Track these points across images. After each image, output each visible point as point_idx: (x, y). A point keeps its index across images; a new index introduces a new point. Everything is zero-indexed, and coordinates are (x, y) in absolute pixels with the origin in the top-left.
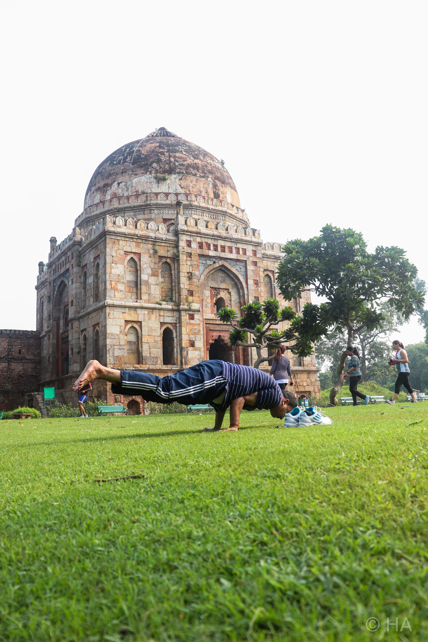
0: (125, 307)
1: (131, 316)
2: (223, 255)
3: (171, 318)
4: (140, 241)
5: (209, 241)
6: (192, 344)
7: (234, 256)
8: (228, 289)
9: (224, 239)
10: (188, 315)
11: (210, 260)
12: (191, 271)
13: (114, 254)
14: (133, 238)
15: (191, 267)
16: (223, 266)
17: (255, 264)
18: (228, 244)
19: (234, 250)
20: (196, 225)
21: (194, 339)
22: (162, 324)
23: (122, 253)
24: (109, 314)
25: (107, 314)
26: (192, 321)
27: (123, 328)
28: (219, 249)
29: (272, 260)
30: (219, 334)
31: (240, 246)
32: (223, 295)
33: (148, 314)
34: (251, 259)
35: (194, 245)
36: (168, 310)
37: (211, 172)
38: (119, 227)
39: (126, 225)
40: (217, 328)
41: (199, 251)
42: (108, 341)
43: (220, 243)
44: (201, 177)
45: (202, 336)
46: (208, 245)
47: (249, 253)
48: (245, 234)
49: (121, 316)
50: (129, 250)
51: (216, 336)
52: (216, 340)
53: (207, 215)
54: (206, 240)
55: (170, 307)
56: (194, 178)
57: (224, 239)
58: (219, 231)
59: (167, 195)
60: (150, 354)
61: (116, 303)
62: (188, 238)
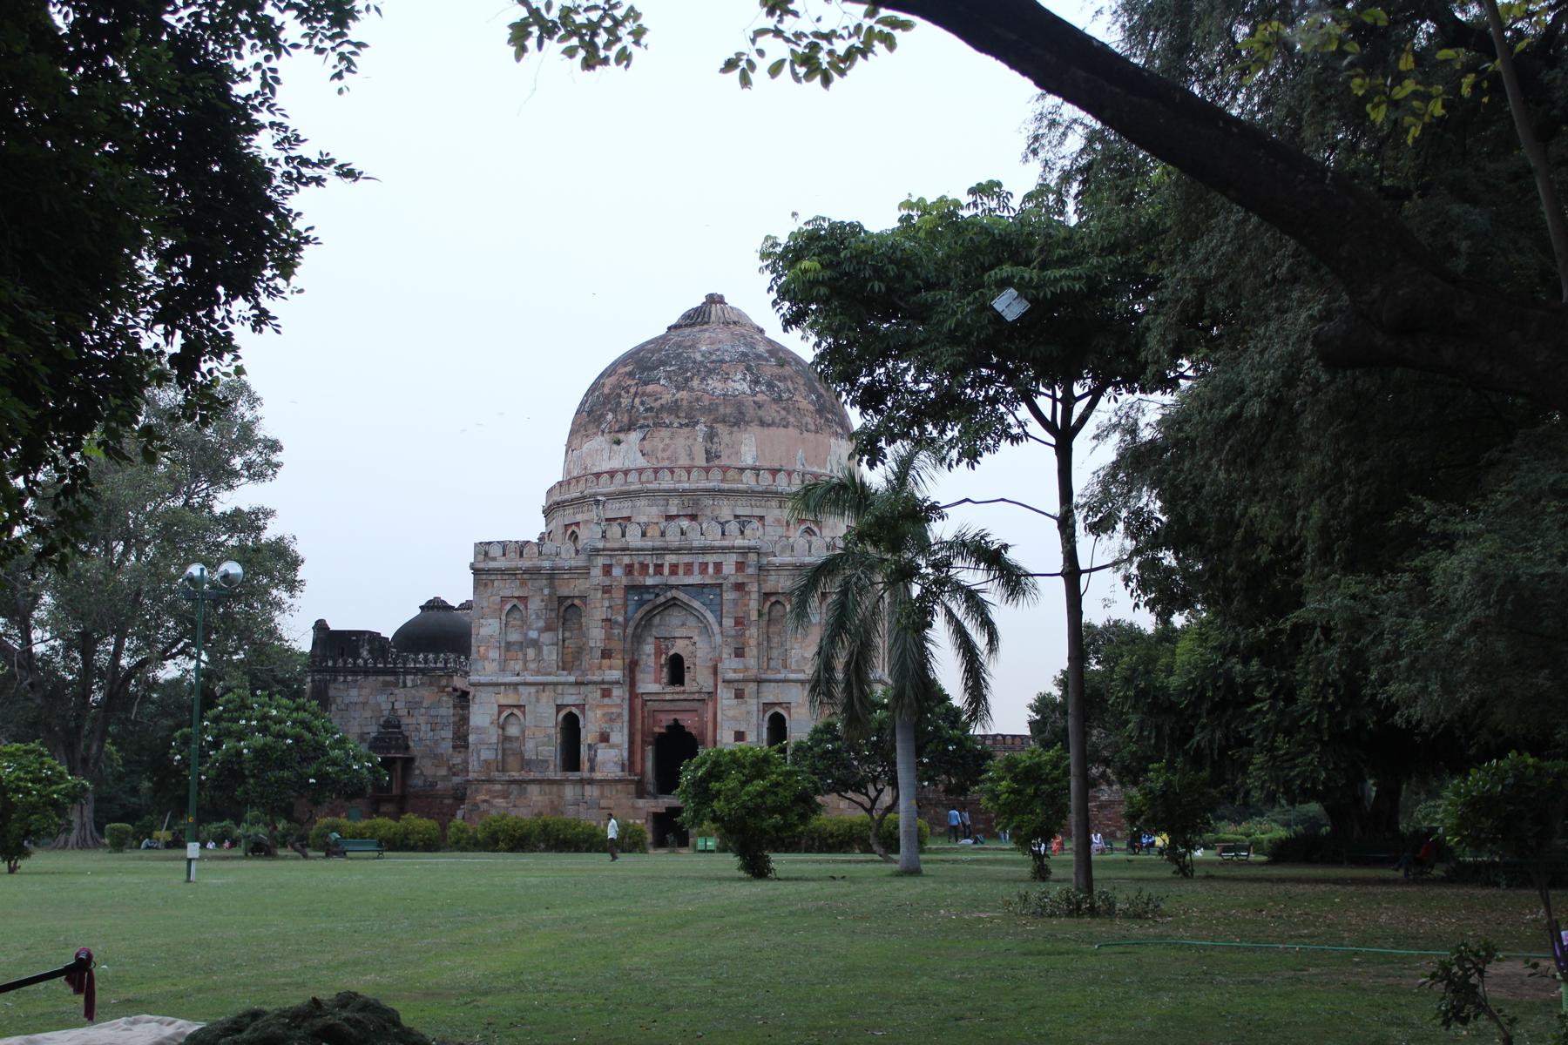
0: (498, 685)
1: (508, 698)
2: (673, 580)
5: (648, 560)
6: (604, 738)
7: (696, 579)
9: (677, 551)
13: (485, 604)
16: (674, 598)
17: (739, 587)
18: (687, 559)
19: (696, 569)
20: (623, 535)
22: (559, 708)
26: (606, 701)
28: (666, 571)
30: (673, 716)
31: (711, 559)
32: (680, 647)
34: (732, 580)
35: (617, 571)
36: (571, 684)
37: (703, 410)
38: (494, 559)
41: (625, 581)
42: (472, 738)
43: (670, 559)
44: (681, 425)
45: (626, 725)
46: (644, 567)
47: (729, 568)
48: (723, 533)
50: (507, 593)
55: (572, 679)
56: (665, 433)
57: (677, 551)
59: (612, 474)
61: (483, 679)
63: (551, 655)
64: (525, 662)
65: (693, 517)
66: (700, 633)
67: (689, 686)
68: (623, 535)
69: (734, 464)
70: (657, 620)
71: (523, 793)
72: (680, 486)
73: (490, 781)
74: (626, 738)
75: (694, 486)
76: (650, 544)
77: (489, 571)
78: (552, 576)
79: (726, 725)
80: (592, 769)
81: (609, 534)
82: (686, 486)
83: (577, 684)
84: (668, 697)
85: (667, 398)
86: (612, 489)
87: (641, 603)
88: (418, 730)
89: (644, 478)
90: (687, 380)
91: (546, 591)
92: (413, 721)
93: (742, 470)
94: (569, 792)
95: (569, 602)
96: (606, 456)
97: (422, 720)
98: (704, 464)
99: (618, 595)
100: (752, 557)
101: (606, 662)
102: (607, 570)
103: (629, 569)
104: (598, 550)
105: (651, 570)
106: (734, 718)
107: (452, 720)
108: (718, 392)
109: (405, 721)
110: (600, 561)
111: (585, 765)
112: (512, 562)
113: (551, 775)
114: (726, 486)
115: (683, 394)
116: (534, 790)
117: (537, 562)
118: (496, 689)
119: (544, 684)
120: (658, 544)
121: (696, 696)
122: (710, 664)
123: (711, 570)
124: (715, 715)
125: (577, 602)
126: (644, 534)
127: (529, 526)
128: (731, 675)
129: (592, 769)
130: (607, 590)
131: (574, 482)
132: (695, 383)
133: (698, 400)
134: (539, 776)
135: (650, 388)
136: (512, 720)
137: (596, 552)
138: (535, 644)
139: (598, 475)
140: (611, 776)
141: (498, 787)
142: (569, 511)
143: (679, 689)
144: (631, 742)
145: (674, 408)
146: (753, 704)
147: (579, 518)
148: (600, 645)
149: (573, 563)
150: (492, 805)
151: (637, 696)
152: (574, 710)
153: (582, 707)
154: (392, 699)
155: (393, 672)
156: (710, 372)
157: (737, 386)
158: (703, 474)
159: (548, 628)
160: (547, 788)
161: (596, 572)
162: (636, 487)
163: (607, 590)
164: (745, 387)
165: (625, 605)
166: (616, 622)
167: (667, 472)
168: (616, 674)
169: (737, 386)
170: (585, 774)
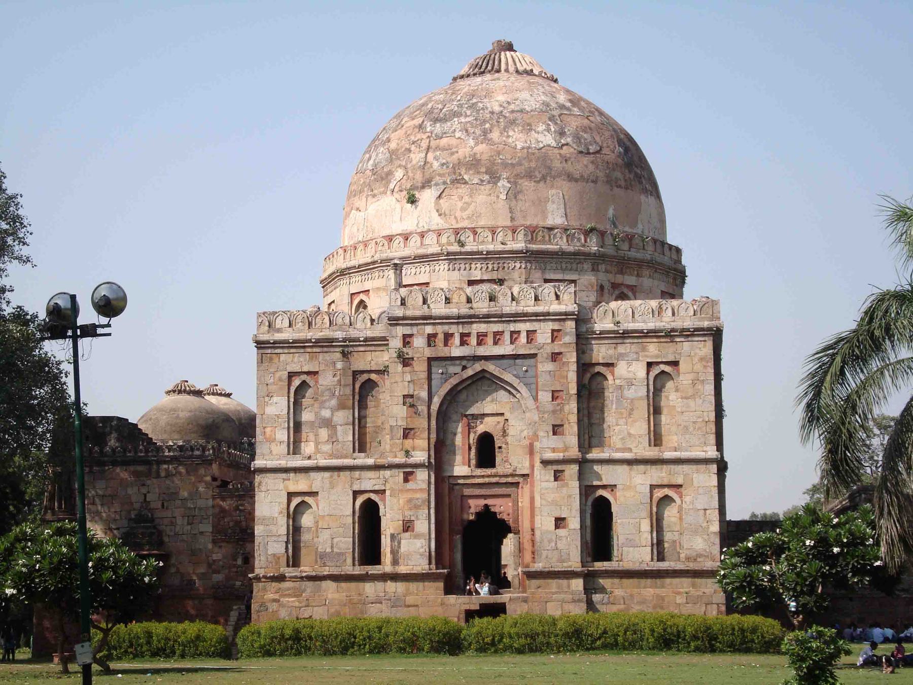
0: (286, 470)
1: (300, 484)
2: (482, 351)
3: (373, 482)
4: (318, 350)
6: (407, 526)
7: (505, 349)
8: (502, 414)
9: (486, 318)
10: (402, 475)
11: (455, 365)
12: (411, 393)
14: (304, 347)
15: (411, 385)
16: (483, 371)
17: (555, 357)
22: (356, 494)
23: (285, 375)
24: (260, 484)
25: (256, 484)
26: (410, 485)
27: (286, 506)
28: (473, 340)
29: (610, 341)
30: (482, 502)
31: (523, 327)
33: (331, 477)
34: (549, 349)
35: (419, 342)
39: (290, 325)
40: (478, 492)
41: (428, 352)
42: (258, 530)
43: (477, 328)
45: (433, 511)
48: (536, 299)
49: (281, 486)
50: (297, 369)
51: (476, 506)
52: (477, 514)
53: (479, 266)
54: (446, 328)
55: (370, 461)
56: (463, 190)
57: (486, 318)
58: (475, 305)
59: (406, 237)
60: (332, 547)
61: (270, 464)
62: (407, 330)
63: (346, 436)
64: (317, 444)
65: (501, 282)
66: (512, 409)
67: (500, 469)
68: (425, 301)
69: (541, 224)
70: (463, 396)
71: (319, 589)
72: (482, 248)
73: (281, 578)
75: (500, 247)
76: (453, 311)
77: (276, 344)
78: (347, 348)
81: (409, 302)
82: (491, 247)
83: (377, 467)
85: (464, 152)
86: (407, 252)
87: (446, 377)
88: (173, 524)
89: (444, 240)
90: (485, 133)
91: (339, 365)
92: (169, 514)
93: (551, 229)
94: (370, 589)
95: (365, 377)
96: (397, 218)
97: (178, 513)
98: (509, 223)
99: (420, 367)
100: (570, 325)
101: (408, 443)
102: (407, 340)
103: (431, 338)
104: (398, 319)
105: (457, 340)
106: (554, 503)
107: (210, 512)
108: (519, 147)
109: (158, 514)
110: (400, 331)
112: (301, 333)
113: (349, 568)
114: (534, 247)
115: (482, 148)
116: (329, 585)
117: (327, 333)
118: (284, 475)
120: (464, 311)
121: (510, 480)
122: (527, 442)
123: (523, 339)
125: (373, 376)
126: (448, 301)
127: (306, 296)
128: (550, 455)
129: (395, 562)
130: (406, 362)
131: (361, 247)
132: (495, 135)
133: (499, 153)
134: (335, 571)
135: (444, 142)
137: (394, 321)
138: (327, 423)
139: (390, 238)
140: (417, 570)
142: (356, 278)
143: (489, 471)
145: (474, 163)
146: (574, 486)
147: (367, 285)
148: (402, 423)
149: (370, 334)
150: (283, 606)
151: (443, 479)
152: (373, 497)
154: (144, 490)
155: (148, 463)
156: (513, 122)
157: (541, 137)
159: (342, 406)
160: (343, 585)
162: (435, 249)
164: (549, 139)
165: (429, 379)
166: (419, 398)
167: (469, 233)
168: (420, 456)
169: (541, 137)
170: (387, 566)
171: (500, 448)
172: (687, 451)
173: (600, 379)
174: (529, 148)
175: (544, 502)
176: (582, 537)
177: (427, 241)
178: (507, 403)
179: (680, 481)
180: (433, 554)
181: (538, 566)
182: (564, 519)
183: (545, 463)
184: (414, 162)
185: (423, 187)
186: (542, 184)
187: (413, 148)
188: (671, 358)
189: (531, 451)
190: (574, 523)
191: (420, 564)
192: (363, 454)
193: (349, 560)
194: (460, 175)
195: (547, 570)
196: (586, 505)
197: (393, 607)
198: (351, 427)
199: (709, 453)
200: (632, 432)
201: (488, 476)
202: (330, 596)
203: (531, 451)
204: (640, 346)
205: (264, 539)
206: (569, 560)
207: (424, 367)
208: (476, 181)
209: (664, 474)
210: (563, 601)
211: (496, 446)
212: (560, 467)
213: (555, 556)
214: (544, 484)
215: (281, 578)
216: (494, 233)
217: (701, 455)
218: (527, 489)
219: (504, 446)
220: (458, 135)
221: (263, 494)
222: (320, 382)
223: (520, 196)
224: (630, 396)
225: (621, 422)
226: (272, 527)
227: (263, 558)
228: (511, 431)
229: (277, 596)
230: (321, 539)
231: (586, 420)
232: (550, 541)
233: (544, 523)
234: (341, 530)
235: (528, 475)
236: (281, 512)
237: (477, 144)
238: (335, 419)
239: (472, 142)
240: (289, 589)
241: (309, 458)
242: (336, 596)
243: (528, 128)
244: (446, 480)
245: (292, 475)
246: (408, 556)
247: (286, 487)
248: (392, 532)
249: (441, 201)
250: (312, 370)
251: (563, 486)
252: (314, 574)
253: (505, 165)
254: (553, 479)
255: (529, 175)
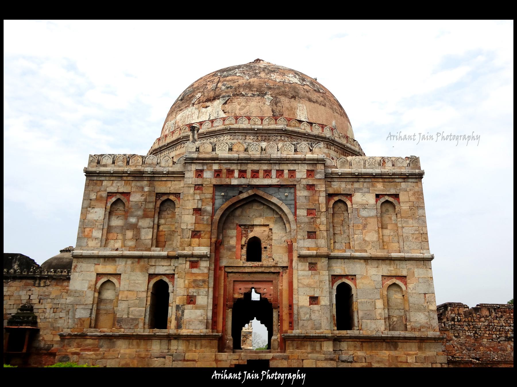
0: (99, 257)
3: (166, 268)
6: (191, 300)
8: (268, 225)
21: (195, 294)
22: (151, 276)
24: (76, 266)
25: (73, 267)
27: (93, 283)
45: (211, 290)
55: (164, 253)
56: (241, 99)
59: (201, 123)
63: (147, 235)
64: (124, 240)
70: (238, 212)
71: (113, 345)
72: (253, 127)
74: (211, 301)
75: (266, 127)
79: (302, 291)
80: (179, 326)
83: (169, 258)
84: (247, 270)
89: (227, 122)
93: (300, 122)
94: (156, 347)
106: (309, 286)
108: (278, 81)
111: (172, 324)
118: (96, 261)
119: (140, 258)
124: (291, 284)
129: (179, 326)
133: (265, 83)
134: (128, 332)
136: (108, 286)
140: (196, 332)
141: (89, 341)
143: (256, 264)
144: (215, 306)
151: (220, 268)
153: (171, 276)
158: (273, 122)
161: (190, 175)
162: (222, 127)
163: (198, 187)
171: (265, 248)
172: (408, 253)
173: (340, 205)
174: (284, 82)
175: (300, 285)
176: (331, 311)
177: (215, 124)
178: (272, 218)
179: (404, 273)
180: (210, 321)
181: (296, 332)
182: (317, 298)
183: (302, 257)
184: (209, 88)
185: (214, 99)
186: (293, 100)
187: (208, 83)
188: (393, 192)
189: (290, 249)
190: (325, 301)
191: (200, 329)
192: (159, 249)
193: (141, 325)
194: (239, 92)
195: (303, 335)
196: (332, 289)
197: (174, 361)
198: (152, 230)
199: (426, 254)
200: (367, 239)
201: (256, 267)
202: (122, 351)
203: (290, 249)
204: (371, 184)
205: (73, 306)
206: (320, 328)
207: (211, 190)
208: (249, 95)
209: (392, 269)
210: (317, 360)
211: (263, 246)
212: (313, 261)
213: (309, 325)
214: (300, 273)
215: (83, 336)
216: (262, 120)
217: (420, 256)
218: (285, 277)
219: (268, 247)
220: (238, 75)
221: (76, 274)
222: (132, 199)
223: (279, 104)
224: (364, 215)
225: (358, 232)
226: (80, 298)
227: (70, 321)
228: (274, 237)
229: (78, 350)
230: (119, 308)
231: (331, 230)
232: (305, 314)
233: (302, 300)
234: (137, 301)
235: (287, 267)
236: (89, 288)
237: (250, 78)
238: (140, 224)
239: (247, 77)
240: (90, 345)
241: (117, 250)
242: (128, 351)
243: (283, 74)
244: (223, 268)
245: (102, 260)
246: (190, 322)
247: (96, 270)
248: (177, 303)
249: (226, 106)
250: (125, 191)
251: (315, 274)
252: (111, 334)
253: (270, 88)
254: (307, 268)
255: (284, 94)
